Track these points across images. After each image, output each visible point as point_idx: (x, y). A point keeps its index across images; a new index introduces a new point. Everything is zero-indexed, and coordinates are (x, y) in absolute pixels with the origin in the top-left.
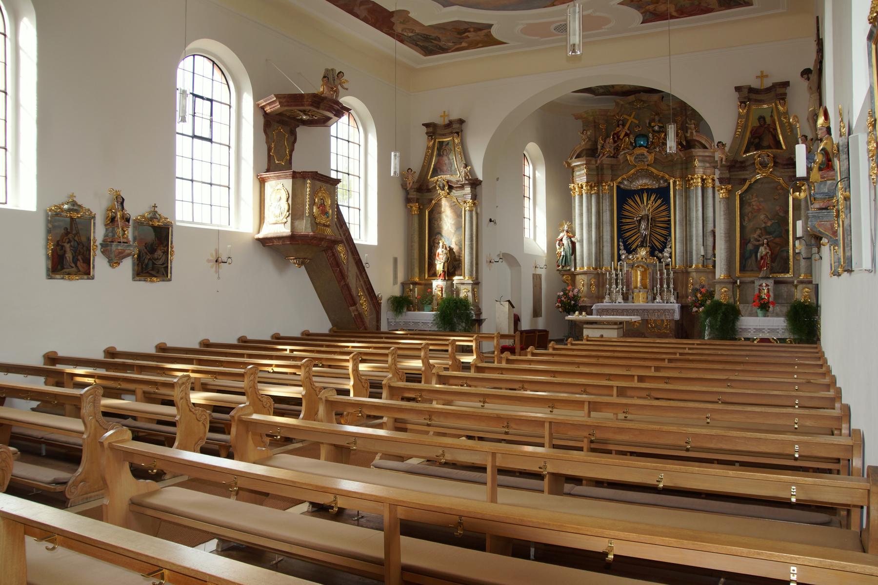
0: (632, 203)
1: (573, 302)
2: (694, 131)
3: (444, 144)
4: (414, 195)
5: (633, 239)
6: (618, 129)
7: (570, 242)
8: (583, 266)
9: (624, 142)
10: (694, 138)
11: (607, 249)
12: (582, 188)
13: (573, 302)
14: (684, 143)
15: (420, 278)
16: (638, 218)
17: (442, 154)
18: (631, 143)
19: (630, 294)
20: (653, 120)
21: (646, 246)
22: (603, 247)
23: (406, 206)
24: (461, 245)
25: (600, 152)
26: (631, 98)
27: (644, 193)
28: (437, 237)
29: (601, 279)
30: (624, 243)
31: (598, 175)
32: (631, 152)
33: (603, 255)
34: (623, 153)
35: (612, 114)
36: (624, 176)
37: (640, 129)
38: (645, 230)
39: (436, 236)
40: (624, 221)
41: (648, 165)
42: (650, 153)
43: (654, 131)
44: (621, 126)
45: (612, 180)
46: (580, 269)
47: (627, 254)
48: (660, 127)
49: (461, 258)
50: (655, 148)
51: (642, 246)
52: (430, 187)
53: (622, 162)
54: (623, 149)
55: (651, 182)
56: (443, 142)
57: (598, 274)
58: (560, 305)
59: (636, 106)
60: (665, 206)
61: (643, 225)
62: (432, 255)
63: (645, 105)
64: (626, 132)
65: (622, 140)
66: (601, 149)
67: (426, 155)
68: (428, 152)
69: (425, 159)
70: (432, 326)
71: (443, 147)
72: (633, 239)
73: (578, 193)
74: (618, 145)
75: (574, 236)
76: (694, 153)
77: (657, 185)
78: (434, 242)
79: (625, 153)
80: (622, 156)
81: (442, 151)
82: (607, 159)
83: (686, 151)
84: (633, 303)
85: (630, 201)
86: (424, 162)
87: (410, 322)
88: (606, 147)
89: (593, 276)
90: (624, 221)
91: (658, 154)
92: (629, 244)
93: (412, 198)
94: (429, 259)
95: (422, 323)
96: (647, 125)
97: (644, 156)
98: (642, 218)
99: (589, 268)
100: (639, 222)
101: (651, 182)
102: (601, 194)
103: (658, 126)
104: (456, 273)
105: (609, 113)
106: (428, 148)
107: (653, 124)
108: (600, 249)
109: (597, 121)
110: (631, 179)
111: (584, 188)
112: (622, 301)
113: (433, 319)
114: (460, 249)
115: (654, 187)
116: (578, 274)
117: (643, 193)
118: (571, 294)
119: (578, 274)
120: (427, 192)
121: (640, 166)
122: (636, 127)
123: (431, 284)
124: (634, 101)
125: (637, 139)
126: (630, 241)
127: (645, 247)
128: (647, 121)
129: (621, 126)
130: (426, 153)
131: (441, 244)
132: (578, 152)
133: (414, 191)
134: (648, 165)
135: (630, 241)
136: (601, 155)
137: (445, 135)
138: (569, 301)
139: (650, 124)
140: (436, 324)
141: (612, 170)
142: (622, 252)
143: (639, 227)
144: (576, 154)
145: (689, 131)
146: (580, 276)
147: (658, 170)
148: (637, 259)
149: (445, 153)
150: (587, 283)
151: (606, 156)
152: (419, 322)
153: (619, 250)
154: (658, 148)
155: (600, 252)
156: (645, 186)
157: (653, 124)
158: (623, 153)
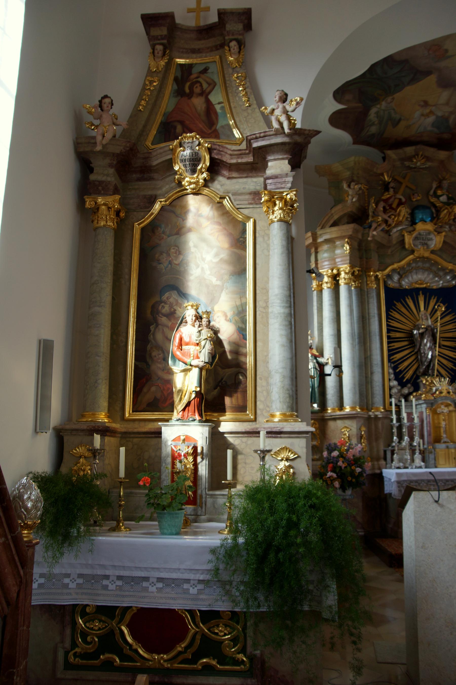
0: (403, 310)
1: (358, 470)
3: (195, 71)
4: (108, 175)
5: (406, 364)
6: (386, 196)
7: (317, 365)
8: (341, 406)
9: (399, 215)
11: (377, 378)
12: (338, 274)
13: (358, 470)
15: (110, 415)
16: (421, 331)
17: (187, 90)
19: (431, 452)
20: (440, 187)
21: (433, 375)
22: (372, 373)
23: (81, 204)
24: (244, 322)
25: (372, 222)
26: (410, 150)
27: (419, 294)
28: (164, 298)
29: (373, 427)
30: (395, 368)
31: (361, 258)
33: (372, 388)
35: (379, 172)
36: (395, 266)
37: (419, 198)
38: (430, 348)
39: (162, 293)
40: (393, 335)
42: (439, 233)
44: (391, 190)
45: (379, 271)
46: (333, 410)
47: (399, 388)
48: (449, 198)
49: (242, 359)
51: (425, 373)
52: (155, 163)
53: (394, 242)
55: (431, 276)
56: (190, 66)
57: (369, 418)
58: (335, 475)
59: (416, 163)
60: (450, 316)
61: (427, 342)
62: (149, 347)
63: (429, 164)
64: (400, 200)
65: (395, 210)
67: (144, 89)
68: (151, 82)
69: (140, 98)
70: (200, 592)
71: (192, 77)
72: (406, 364)
73: (329, 285)
75: (322, 355)
77: (441, 282)
78: (155, 311)
80: (397, 234)
81: (188, 84)
84: (436, 467)
85: (399, 305)
86: (138, 103)
87: (107, 577)
89: (362, 421)
90: (393, 335)
91: (450, 234)
92: (401, 372)
93: (101, 182)
94: (137, 358)
95: (160, 580)
96: (432, 192)
98: (426, 329)
99: (353, 408)
100: (422, 335)
101: (431, 276)
102: (366, 290)
104: (227, 400)
106: (150, 73)
108: (366, 377)
110: (402, 273)
111: (343, 275)
112: (423, 464)
113: (210, 566)
114: (242, 331)
115: (435, 287)
116: (335, 419)
117: (418, 294)
118: (350, 455)
119: (335, 419)
120: (139, 180)
121: (421, 251)
123: (158, 434)
124: (414, 157)
125: (417, 211)
126: (402, 367)
127: (429, 375)
130: (145, 84)
131: (190, 314)
132: (336, 217)
133: (111, 166)
134: (433, 252)
135: (402, 367)
136: (374, 225)
137: (201, 52)
138: (353, 467)
139: (435, 192)
140: (223, 584)
142: (395, 383)
143: (420, 345)
144: (331, 222)
146: (339, 422)
147: (445, 260)
148: (441, 393)
149: (197, 90)
150: (357, 434)
152: (146, 579)
153: (390, 380)
154: (447, 227)
155: (367, 383)
156: (421, 284)
157: (439, 192)
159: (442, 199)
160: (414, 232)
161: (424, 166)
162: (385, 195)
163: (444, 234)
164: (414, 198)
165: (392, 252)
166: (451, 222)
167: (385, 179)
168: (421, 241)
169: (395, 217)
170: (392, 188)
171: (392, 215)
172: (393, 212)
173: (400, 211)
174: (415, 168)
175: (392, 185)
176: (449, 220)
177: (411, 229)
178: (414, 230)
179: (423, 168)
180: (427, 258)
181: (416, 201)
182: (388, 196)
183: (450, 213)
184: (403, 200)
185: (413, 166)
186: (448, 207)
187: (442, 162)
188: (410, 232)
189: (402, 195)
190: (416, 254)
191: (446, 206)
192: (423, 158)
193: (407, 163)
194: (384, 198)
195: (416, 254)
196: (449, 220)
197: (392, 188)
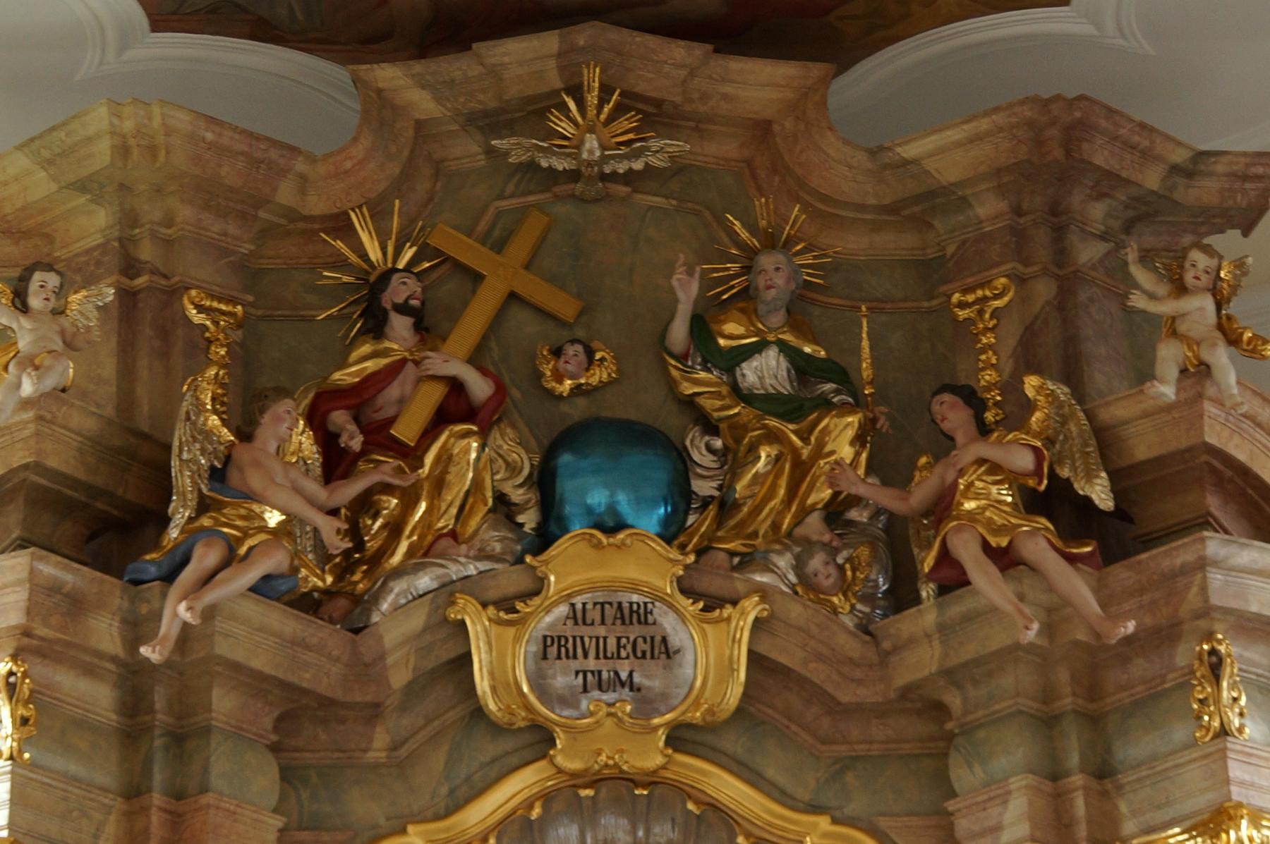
2: (1221, 357)
9: (439, 484)
10: (1211, 439)
14: (1100, 494)
18: (504, 507)
31: (134, 792)
32: (511, 580)
34: (425, 581)
35: (317, 205)
37: (597, 376)
41: (681, 737)
42: (712, 603)
43: (738, 393)
44: (400, 325)
48: (803, 368)
50: (746, 561)
53: (399, 678)
54: (423, 554)
64: (456, 386)
65: (411, 455)
66: (204, 506)
74: (365, 504)
76: (1216, 578)
79: (448, 591)
80: (417, 620)
82: (257, 610)
83: (1121, 574)
88: (255, 481)
91: (796, 611)
96: (679, 333)
97: (634, 631)
103: (784, 347)
105: (285, 194)
107: (732, 332)
109: (146, 252)
122: (557, 352)
125: (566, 459)
128: (687, 292)
129: (400, 325)
134: (681, 737)
136: (205, 557)
139: (701, 328)
141: (288, 775)
145: (1169, 356)
151: (252, 575)
154: (784, 562)
158: (425, 581)
159: (753, 373)
160: (537, 601)
161: (638, 165)
162: (355, 355)
163: (752, 609)
164: (559, 378)
165: (394, 748)
166: (814, 525)
167: (364, 256)
168: (591, 664)
169: (409, 504)
170: (403, 309)
171: (387, 489)
172: (385, 469)
173: (445, 459)
174: (574, 176)
175: (401, 290)
176: (804, 512)
177: (511, 580)
178: (538, 587)
179: (630, 178)
180: (652, 780)
181: (577, 390)
182: (371, 366)
183: (801, 469)
184: (479, 387)
185: (560, 164)
186: (789, 429)
187: (762, 130)
188: (506, 604)
189: (476, 359)
190: (567, 757)
191: (773, 422)
192: (619, 110)
193: (515, 148)
194: (346, 376)
195: (567, 757)
196: (799, 520)
197: (403, 309)
